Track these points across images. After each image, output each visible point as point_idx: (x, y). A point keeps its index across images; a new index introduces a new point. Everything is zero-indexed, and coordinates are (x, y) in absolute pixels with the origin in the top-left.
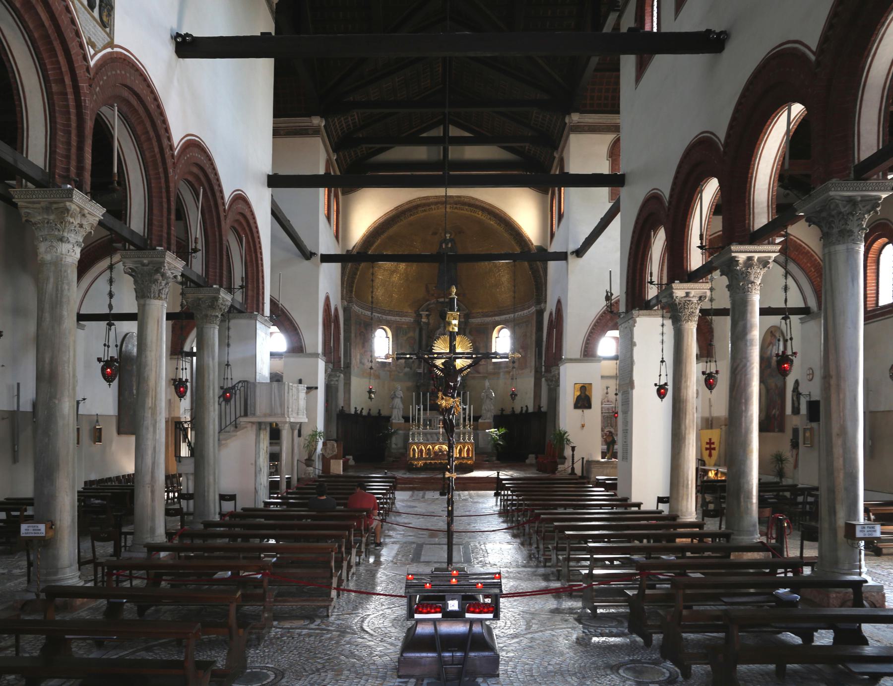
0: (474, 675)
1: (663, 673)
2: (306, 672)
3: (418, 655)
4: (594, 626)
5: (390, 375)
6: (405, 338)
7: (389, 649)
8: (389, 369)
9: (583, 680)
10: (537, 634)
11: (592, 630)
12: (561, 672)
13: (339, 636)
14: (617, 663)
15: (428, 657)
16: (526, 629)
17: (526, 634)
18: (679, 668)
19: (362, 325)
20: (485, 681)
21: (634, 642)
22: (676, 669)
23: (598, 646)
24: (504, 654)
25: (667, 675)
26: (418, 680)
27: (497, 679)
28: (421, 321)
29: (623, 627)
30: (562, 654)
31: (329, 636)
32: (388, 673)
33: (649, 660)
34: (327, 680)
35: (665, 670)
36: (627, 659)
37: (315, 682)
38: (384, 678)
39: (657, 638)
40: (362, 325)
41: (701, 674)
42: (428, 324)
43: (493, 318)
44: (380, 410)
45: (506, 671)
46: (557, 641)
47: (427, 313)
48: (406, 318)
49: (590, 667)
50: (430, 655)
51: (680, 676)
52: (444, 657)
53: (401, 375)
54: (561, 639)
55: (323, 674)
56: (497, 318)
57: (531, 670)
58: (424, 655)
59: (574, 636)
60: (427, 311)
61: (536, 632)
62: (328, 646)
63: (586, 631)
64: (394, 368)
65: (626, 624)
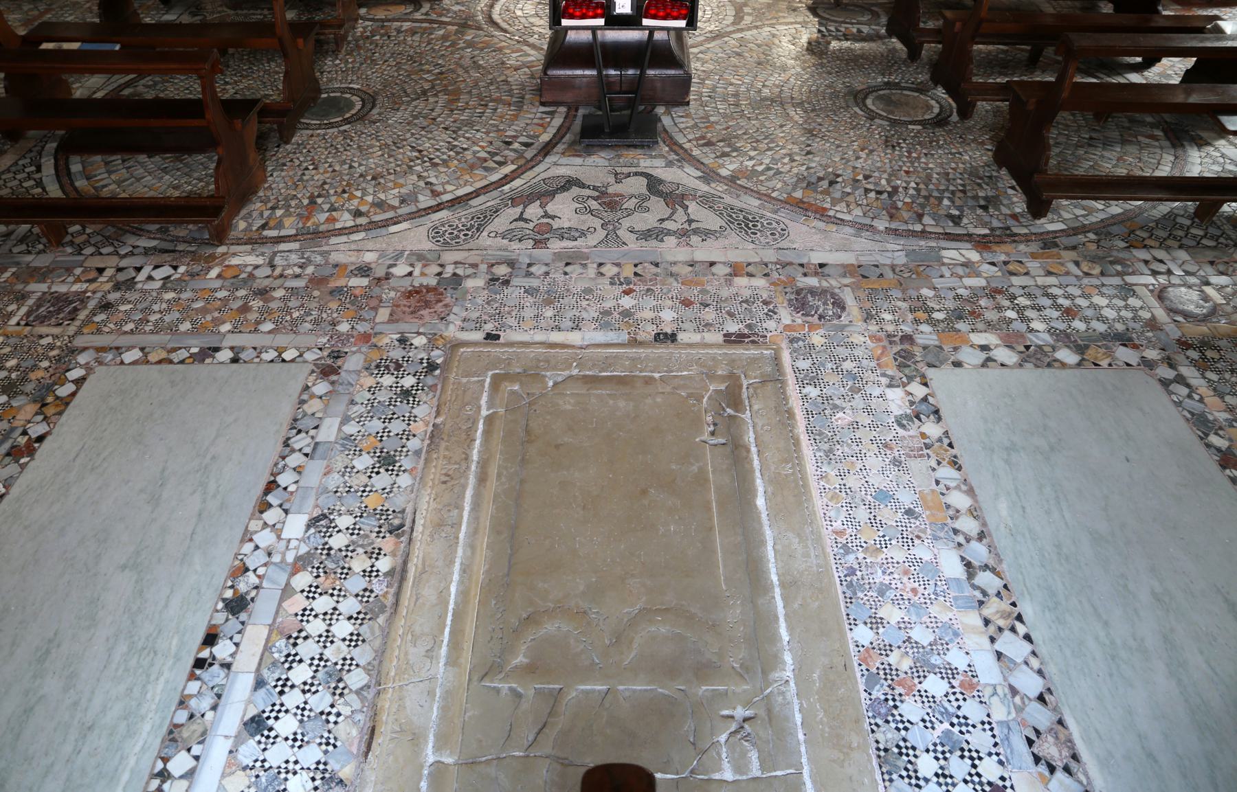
0: (654, 101)
1: (930, 108)
2: (408, 96)
3: (569, 72)
4: (836, 22)
7: (529, 55)
9: (812, 115)
10: (750, 32)
11: (832, 28)
12: (778, 100)
13: (457, 32)
14: (864, 87)
15: (584, 76)
16: (733, 24)
17: (734, 32)
18: (954, 100)
20: (668, 113)
21: (894, 50)
22: (950, 100)
23: (840, 56)
24: (698, 65)
25: (936, 110)
26: (569, 109)
27: (687, 108)
29: (878, 24)
30: (784, 68)
31: (441, 32)
32: (527, 97)
33: (913, 83)
34: (438, 110)
35: (933, 102)
36: (879, 80)
37: (420, 113)
38: (520, 104)
39: (930, 49)
41: (987, 111)
45: (700, 95)
46: (778, 46)
49: (823, 92)
50: (588, 72)
51: (955, 114)
52: (607, 76)
54: (785, 39)
55: (431, 100)
57: (736, 95)
58: (579, 72)
59: (804, 39)
61: (749, 29)
62: (440, 50)
63: (823, 29)
65: (884, 20)
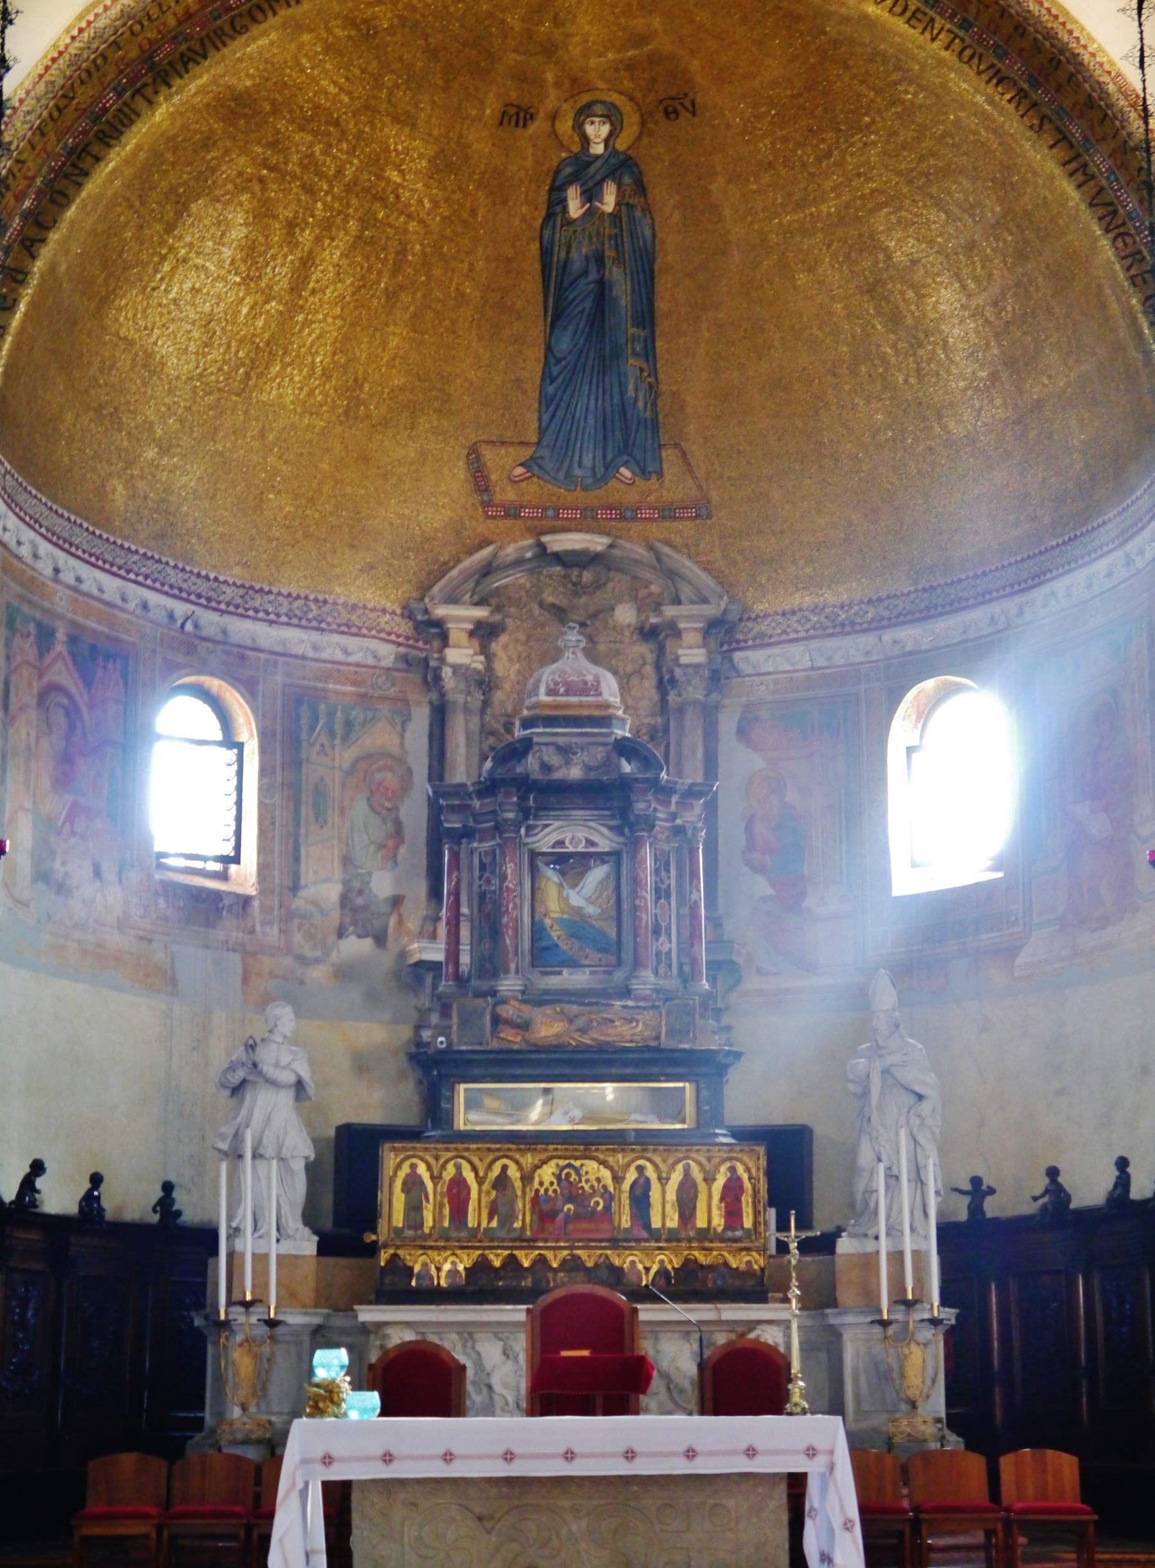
5: (245, 980)
6: (347, 756)
8: (237, 936)
19: (60, 647)
28: (442, 660)
40: (60, 647)
42: (485, 683)
43: (888, 636)
44: (168, 1187)
47: (481, 613)
48: (352, 642)
53: (318, 974)
56: (910, 636)
60: (478, 604)
64: (273, 934)
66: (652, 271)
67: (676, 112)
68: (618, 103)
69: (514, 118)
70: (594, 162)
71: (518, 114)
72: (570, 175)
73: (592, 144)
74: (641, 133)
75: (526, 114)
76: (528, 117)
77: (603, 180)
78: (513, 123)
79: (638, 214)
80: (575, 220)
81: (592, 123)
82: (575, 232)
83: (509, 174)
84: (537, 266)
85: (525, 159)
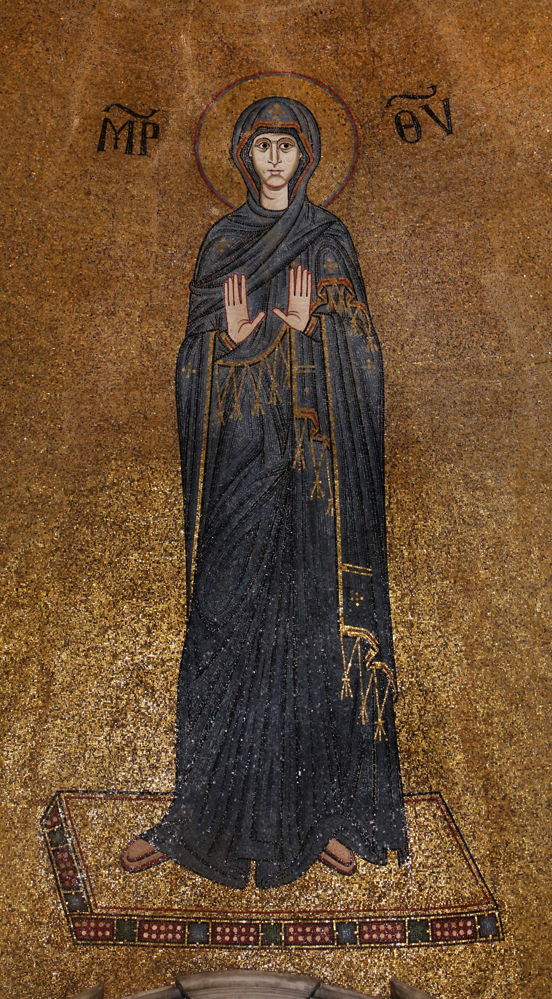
66: (379, 446)
67: (416, 123)
68: (310, 104)
69: (125, 133)
70: (272, 226)
71: (131, 123)
72: (229, 253)
73: (265, 189)
74: (353, 169)
75: (145, 125)
76: (150, 134)
77: (288, 263)
78: (123, 145)
79: (352, 333)
80: (239, 346)
81: (266, 145)
82: (238, 369)
83: (116, 253)
84: (172, 437)
85: (145, 221)
